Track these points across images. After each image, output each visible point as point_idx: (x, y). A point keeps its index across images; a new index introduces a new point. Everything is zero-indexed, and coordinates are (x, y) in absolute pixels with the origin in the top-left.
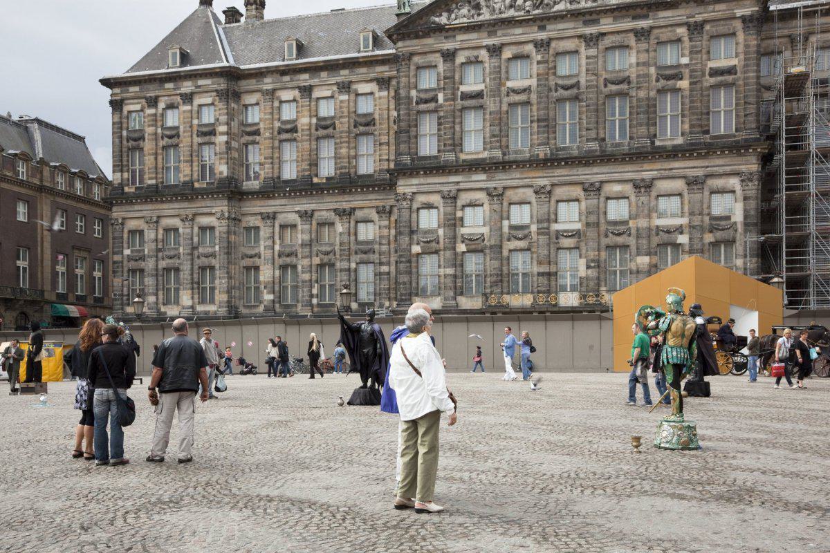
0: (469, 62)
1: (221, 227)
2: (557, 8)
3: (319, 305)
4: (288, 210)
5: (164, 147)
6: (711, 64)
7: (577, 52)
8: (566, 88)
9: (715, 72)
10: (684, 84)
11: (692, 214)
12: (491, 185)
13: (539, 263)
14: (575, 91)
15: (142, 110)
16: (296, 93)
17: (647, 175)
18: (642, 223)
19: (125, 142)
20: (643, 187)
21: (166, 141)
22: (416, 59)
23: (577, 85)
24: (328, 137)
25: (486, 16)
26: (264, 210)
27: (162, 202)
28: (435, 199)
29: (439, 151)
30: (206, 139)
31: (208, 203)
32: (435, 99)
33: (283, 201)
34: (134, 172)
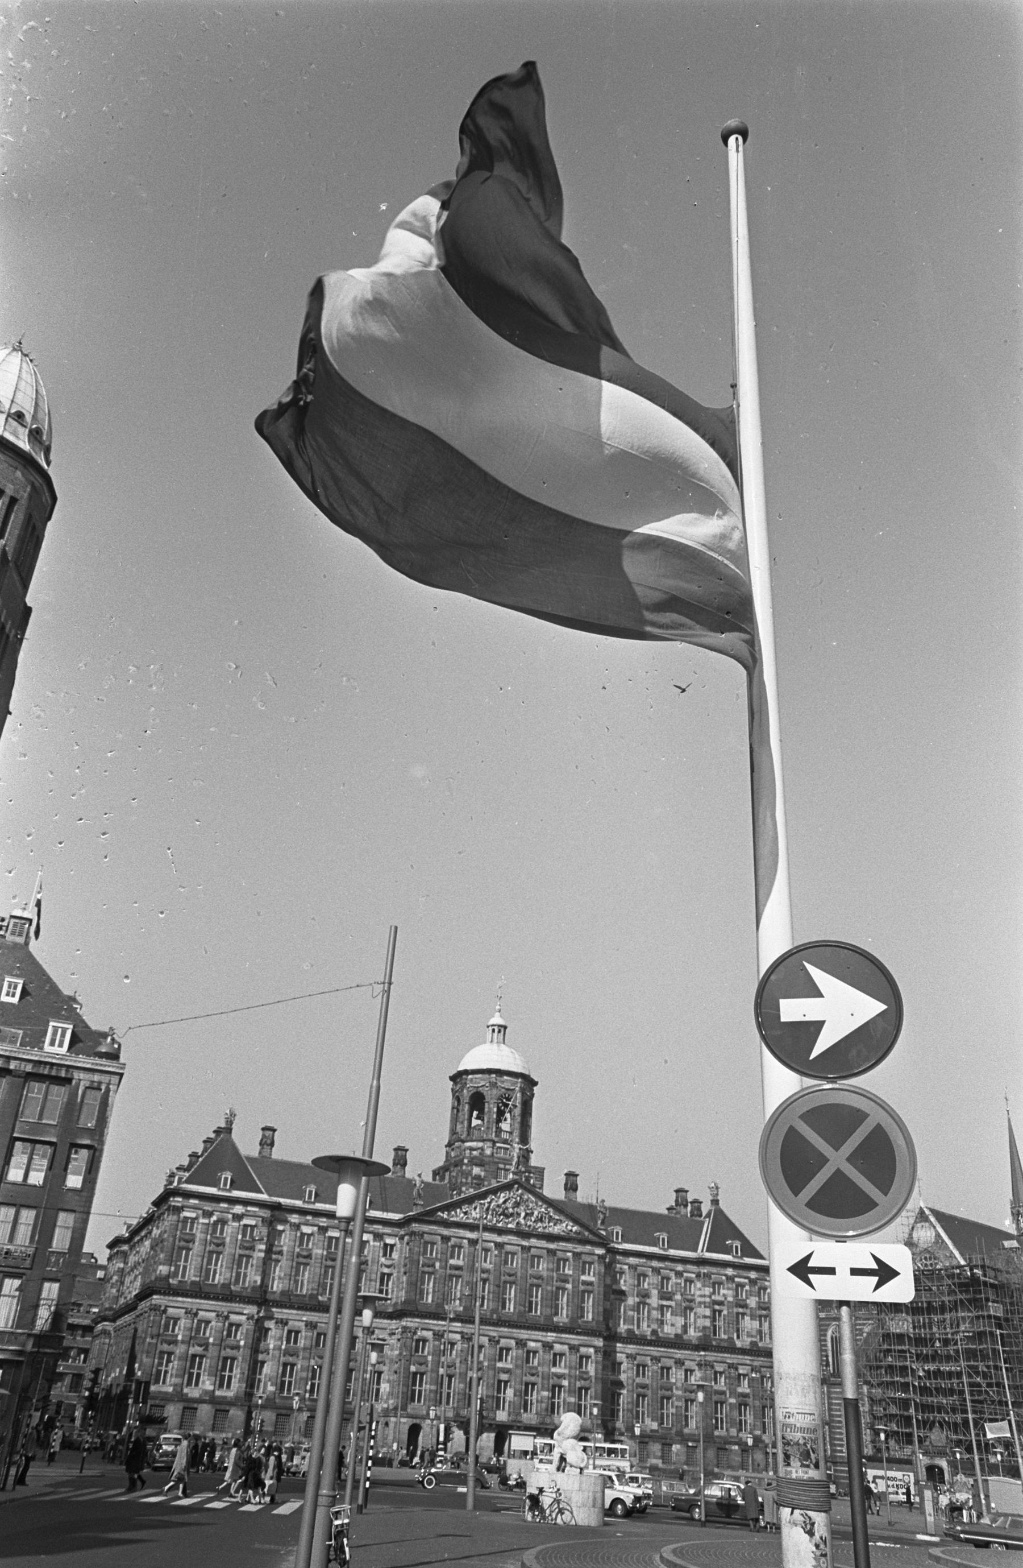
1: (247, 1326)
2: (510, 1226)
3: (310, 1399)
4: (297, 1319)
6: (583, 1278)
8: (510, 1275)
9: (585, 1283)
10: (569, 1286)
11: (570, 1368)
13: (487, 1388)
14: (512, 1278)
15: (196, 1218)
16: (316, 1229)
18: (546, 1369)
20: (548, 1346)
21: (212, 1247)
28: (429, 1335)
30: (247, 1252)
31: (241, 1305)
32: (433, 1266)
33: (294, 1312)
34: (177, 1267)
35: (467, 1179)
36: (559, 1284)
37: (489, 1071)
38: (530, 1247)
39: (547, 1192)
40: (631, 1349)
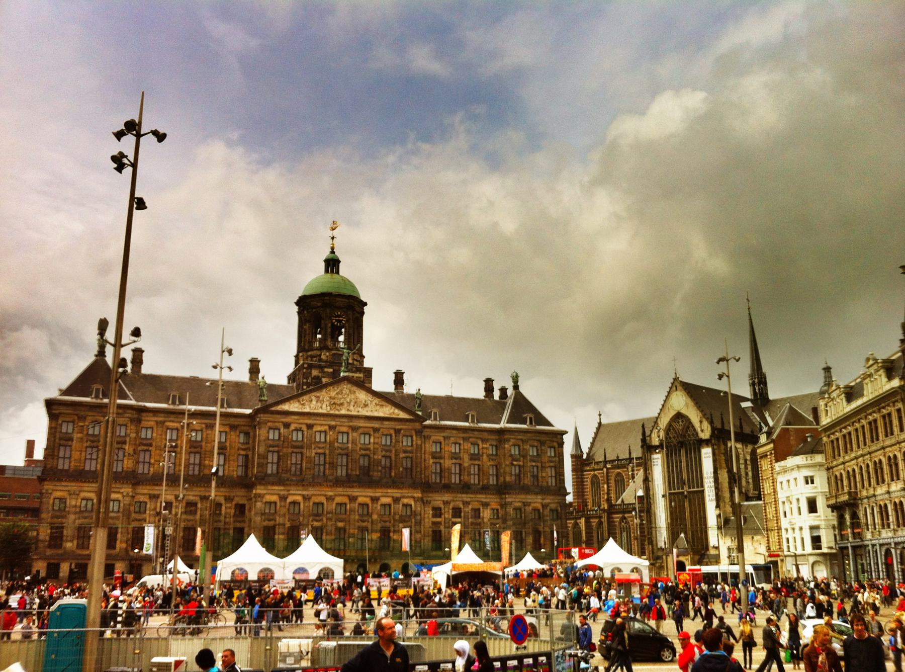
0: (297, 430)
5: (87, 447)
7: (348, 433)
12: (305, 493)
13: (327, 534)
17: (377, 495)
19: (57, 440)
20: (375, 500)
21: (89, 444)
22: (269, 424)
23: (348, 448)
24: (195, 453)
25: (307, 410)
26: (151, 492)
27: (85, 482)
28: (274, 498)
29: (278, 472)
31: (118, 486)
35: (307, 379)
36: (384, 453)
37: (323, 295)
38: (360, 427)
39: (376, 386)
40: (447, 497)
